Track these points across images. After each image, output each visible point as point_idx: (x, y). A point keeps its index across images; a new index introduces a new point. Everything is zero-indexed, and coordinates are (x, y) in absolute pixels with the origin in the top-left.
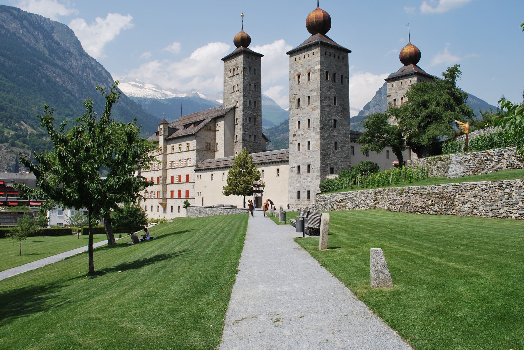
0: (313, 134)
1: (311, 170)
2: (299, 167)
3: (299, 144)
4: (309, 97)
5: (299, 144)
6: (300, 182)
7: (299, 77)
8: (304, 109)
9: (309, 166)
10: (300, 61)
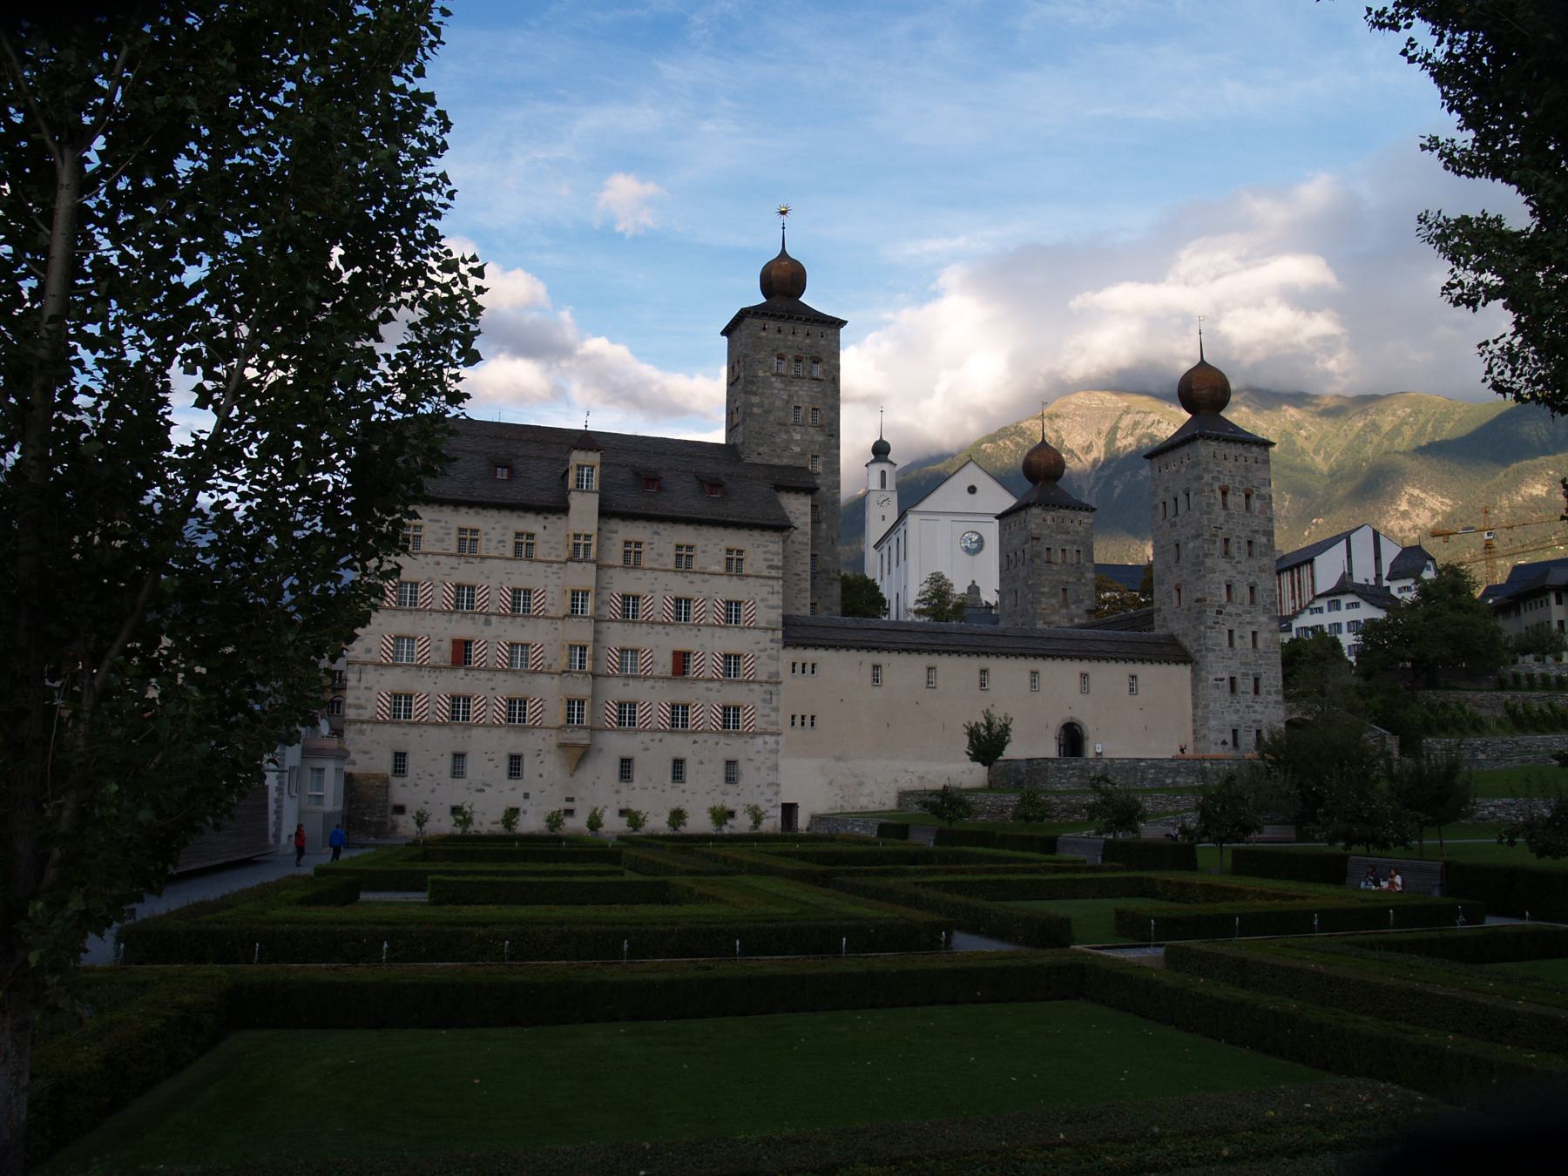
0: (1263, 619)
1: (1263, 690)
2: (1232, 680)
3: (1231, 632)
5: (1231, 632)
6: (1237, 711)
7: (1224, 493)
9: (1256, 680)
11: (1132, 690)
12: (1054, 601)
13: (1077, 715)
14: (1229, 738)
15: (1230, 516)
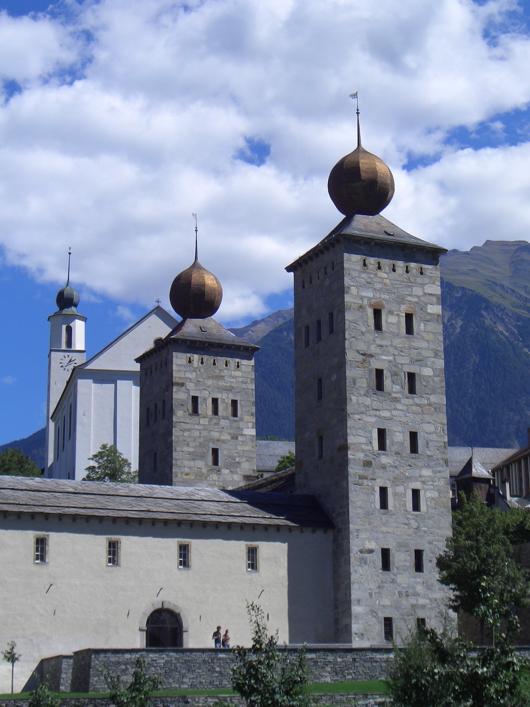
2: (386, 553)
3: (383, 491)
4: (411, 377)
5: (383, 491)
7: (377, 313)
8: (396, 400)
10: (380, 274)
11: (253, 565)
12: (200, 464)
13: (172, 599)
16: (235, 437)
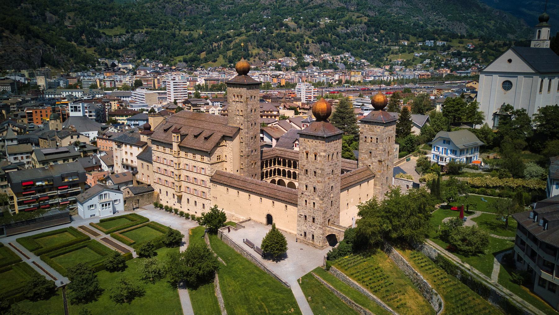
0: (318, 199)
5: (306, 201)
6: (306, 227)
7: (307, 154)
12: (366, 156)
14: (303, 234)
15: (308, 162)
16: (376, 149)
